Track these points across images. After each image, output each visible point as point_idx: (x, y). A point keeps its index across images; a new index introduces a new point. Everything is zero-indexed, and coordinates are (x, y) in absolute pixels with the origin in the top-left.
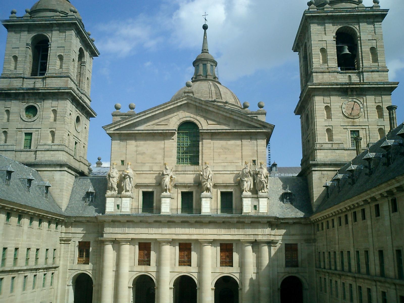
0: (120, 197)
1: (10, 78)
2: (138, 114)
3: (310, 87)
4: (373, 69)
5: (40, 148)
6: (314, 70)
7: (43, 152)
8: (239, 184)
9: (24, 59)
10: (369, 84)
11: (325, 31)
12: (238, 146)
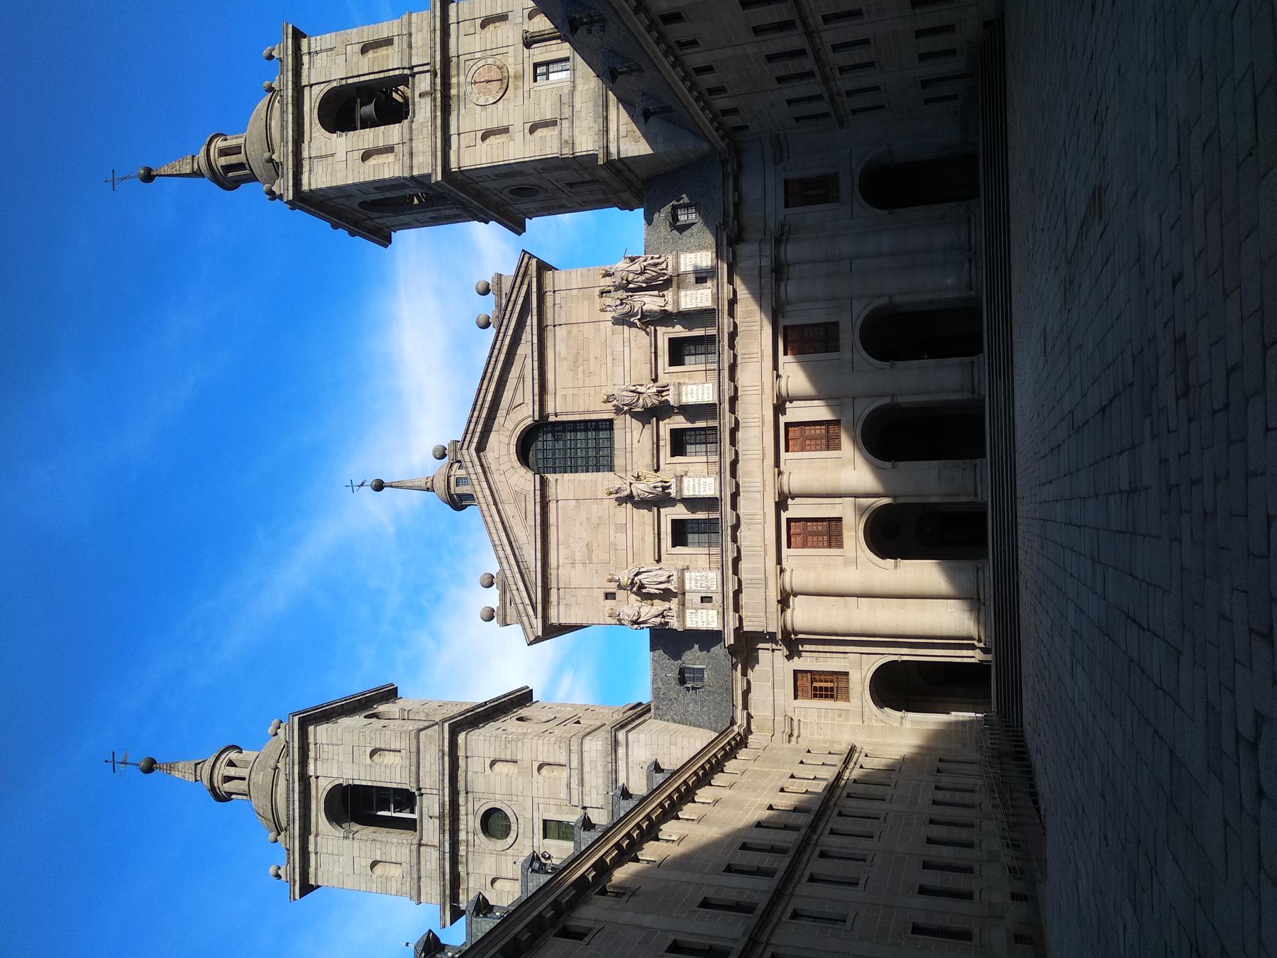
0: (684, 594)
1: (419, 878)
2: (501, 563)
3: (439, 178)
4: (405, 46)
5: (575, 801)
6: (407, 175)
7: (586, 790)
8: (651, 320)
9: (379, 846)
10: (433, 48)
11: (326, 156)
12: (569, 332)
